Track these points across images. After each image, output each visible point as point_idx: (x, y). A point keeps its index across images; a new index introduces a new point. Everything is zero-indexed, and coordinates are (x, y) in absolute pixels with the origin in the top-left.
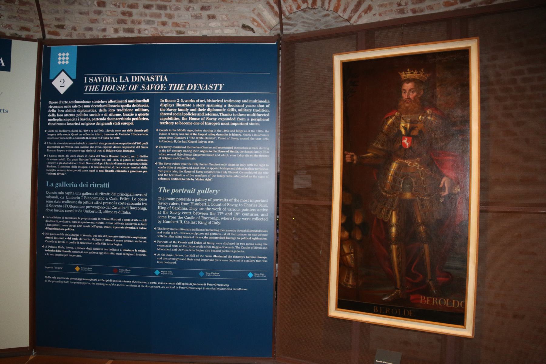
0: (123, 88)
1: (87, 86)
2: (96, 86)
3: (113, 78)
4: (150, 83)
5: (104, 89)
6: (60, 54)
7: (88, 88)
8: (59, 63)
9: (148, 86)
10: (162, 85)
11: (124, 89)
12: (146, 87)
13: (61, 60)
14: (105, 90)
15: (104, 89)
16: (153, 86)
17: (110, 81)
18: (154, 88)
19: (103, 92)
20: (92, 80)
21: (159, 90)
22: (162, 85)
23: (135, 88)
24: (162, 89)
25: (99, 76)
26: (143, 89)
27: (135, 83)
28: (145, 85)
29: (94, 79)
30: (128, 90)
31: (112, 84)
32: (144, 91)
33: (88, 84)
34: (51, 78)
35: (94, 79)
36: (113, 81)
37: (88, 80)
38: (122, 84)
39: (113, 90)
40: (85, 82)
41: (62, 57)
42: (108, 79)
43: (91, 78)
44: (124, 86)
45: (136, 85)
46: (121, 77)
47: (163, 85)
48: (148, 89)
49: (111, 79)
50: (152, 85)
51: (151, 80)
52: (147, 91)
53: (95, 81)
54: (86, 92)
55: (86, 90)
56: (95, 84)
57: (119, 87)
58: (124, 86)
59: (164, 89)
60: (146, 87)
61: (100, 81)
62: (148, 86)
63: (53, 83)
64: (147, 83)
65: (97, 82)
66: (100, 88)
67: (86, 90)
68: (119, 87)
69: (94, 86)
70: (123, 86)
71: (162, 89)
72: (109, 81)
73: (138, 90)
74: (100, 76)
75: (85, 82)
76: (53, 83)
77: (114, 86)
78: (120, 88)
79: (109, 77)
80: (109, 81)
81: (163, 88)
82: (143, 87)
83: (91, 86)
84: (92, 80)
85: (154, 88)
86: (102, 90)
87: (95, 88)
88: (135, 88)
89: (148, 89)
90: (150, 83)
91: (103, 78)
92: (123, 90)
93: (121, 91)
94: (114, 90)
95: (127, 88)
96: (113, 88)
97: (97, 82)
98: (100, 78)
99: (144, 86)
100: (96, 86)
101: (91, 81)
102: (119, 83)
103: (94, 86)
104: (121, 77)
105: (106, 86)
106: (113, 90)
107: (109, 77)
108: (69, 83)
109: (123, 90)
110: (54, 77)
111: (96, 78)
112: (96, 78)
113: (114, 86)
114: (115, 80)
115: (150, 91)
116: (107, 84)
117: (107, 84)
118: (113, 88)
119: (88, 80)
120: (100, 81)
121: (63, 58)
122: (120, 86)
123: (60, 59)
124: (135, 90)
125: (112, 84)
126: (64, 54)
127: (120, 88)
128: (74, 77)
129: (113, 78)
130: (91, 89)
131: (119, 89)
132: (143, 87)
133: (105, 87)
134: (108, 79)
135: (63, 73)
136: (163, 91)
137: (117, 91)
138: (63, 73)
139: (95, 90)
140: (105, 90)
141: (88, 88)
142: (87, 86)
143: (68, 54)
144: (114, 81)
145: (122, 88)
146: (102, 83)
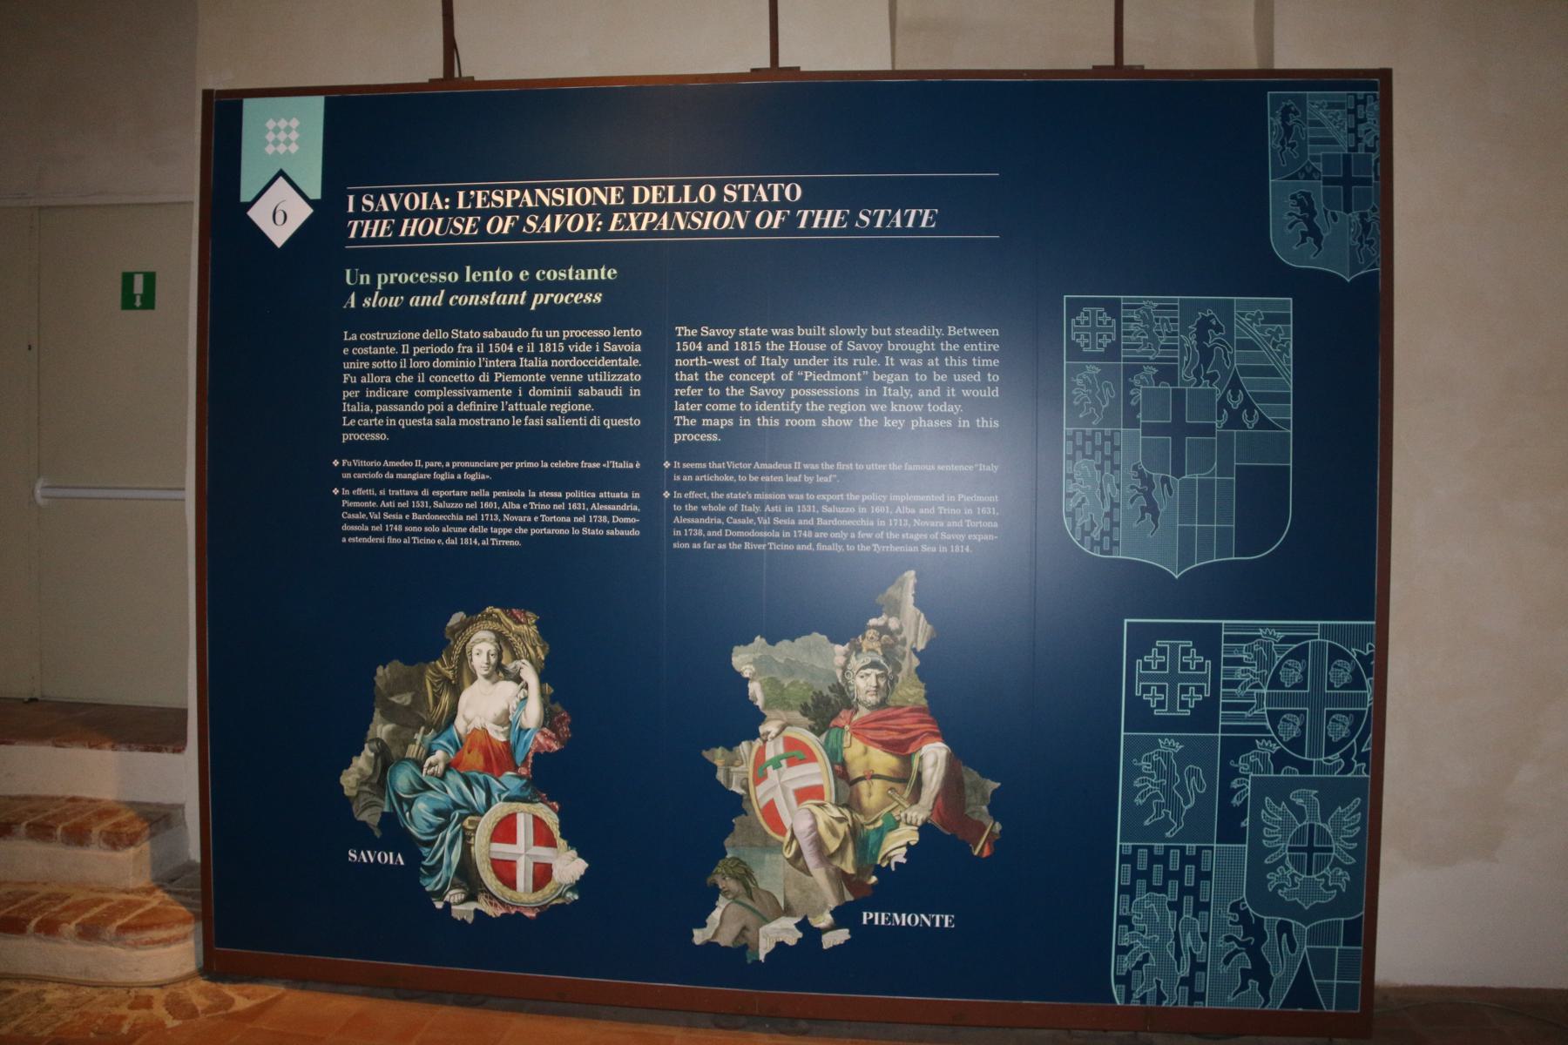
0: (467, 227)
1: (356, 223)
2: (385, 222)
3: (437, 197)
4: (553, 211)
5: (408, 231)
6: (271, 124)
7: (360, 229)
8: (270, 149)
9: (548, 220)
10: (590, 216)
11: (472, 230)
12: (539, 223)
13: (276, 143)
14: (412, 234)
15: (408, 231)
16: (562, 218)
17: (428, 206)
18: (564, 226)
19: (407, 239)
20: (371, 204)
21: (583, 234)
22: (590, 216)
24: (589, 229)
25: (392, 191)
26: (530, 228)
27: (504, 212)
28: (537, 217)
29: (376, 201)
30: (483, 235)
31: (434, 214)
32: (535, 236)
33: (358, 214)
34: (245, 197)
35: (376, 201)
36: (435, 206)
37: (358, 203)
38: (466, 214)
39: (437, 232)
40: (351, 210)
41: (277, 130)
42: (421, 202)
43: (368, 198)
44: (471, 219)
45: (509, 218)
46: (461, 194)
47: (594, 217)
48: (548, 230)
50: (558, 217)
51: (553, 204)
52: (543, 236)
53: (381, 208)
54: (352, 242)
55: (352, 235)
56: (381, 215)
57: (456, 224)
58: (471, 219)
59: (598, 229)
60: (539, 223)
61: (396, 207)
62: (548, 220)
63: (252, 213)
64: (542, 211)
65: (386, 209)
66: (396, 228)
67: (352, 235)
68: (456, 224)
69: (377, 222)
70: (467, 221)
71: (589, 229)
72: (424, 207)
73: (515, 232)
74: (397, 192)
75: (351, 210)
76: (252, 213)
77: (440, 220)
78: (460, 227)
79: (425, 195)
80: (424, 207)
81: (595, 226)
82: (529, 222)
83: (368, 222)
84: (371, 204)
85: (564, 226)
86: (403, 234)
87: (381, 229)
89: (548, 230)
90: (553, 211)
91: (404, 197)
92: (467, 232)
93: (463, 238)
94: (442, 231)
95: (481, 226)
96: (435, 227)
97: (386, 209)
98: (397, 198)
99: (533, 219)
100: (385, 222)
101: (368, 207)
102: (454, 212)
103: (377, 222)
104: (461, 194)
105: (416, 221)
106: (437, 232)
107: (425, 195)
108: (300, 213)
109: (467, 232)
110: (254, 195)
111: (382, 198)
112: (382, 198)
113: (440, 220)
114: (444, 204)
115: (552, 235)
116: (420, 214)
117: (420, 214)
118: (435, 227)
119: (358, 203)
120: (396, 207)
121: (282, 136)
122: (459, 221)
123: (270, 137)
124: (506, 231)
125: (434, 214)
126: (283, 123)
127: (460, 227)
128: (316, 193)
129: (437, 197)
130: (370, 232)
131: (456, 230)
132: (529, 222)
133: (410, 224)
134: (421, 202)
135: (281, 179)
136: (594, 234)
137: (449, 238)
138: (281, 179)
139: (381, 235)
140: (412, 234)
141: (360, 229)
142: (356, 223)
143: (295, 123)
144: (440, 207)
145: (465, 225)
146: (402, 213)
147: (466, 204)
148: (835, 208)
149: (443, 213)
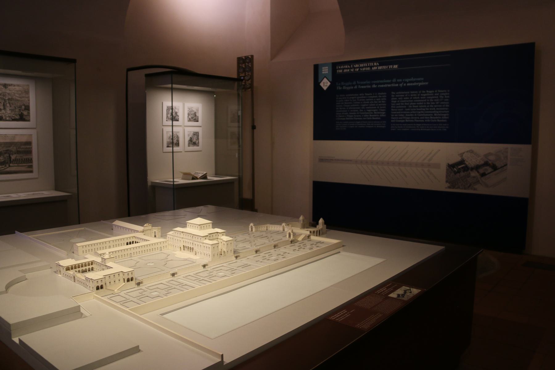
0: (352, 70)
12: (362, 69)
23: (358, 70)
29: (340, 67)
30: (355, 71)
31: (348, 68)
37: (338, 67)
42: (346, 67)
49: (348, 66)
60: (362, 69)
64: (362, 67)
66: (343, 71)
73: (359, 70)
87: (341, 71)
88: (358, 70)
95: (354, 70)
96: (348, 70)
102: (351, 68)
115: (364, 71)
118: (348, 70)
119: (338, 67)
125: (348, 68)
134: (346, 67)
136: (370, 70)
141: (338, 71)
146: (343, 69)
147: (352, 66)
148: (396, 65)
149: (349, 68)
